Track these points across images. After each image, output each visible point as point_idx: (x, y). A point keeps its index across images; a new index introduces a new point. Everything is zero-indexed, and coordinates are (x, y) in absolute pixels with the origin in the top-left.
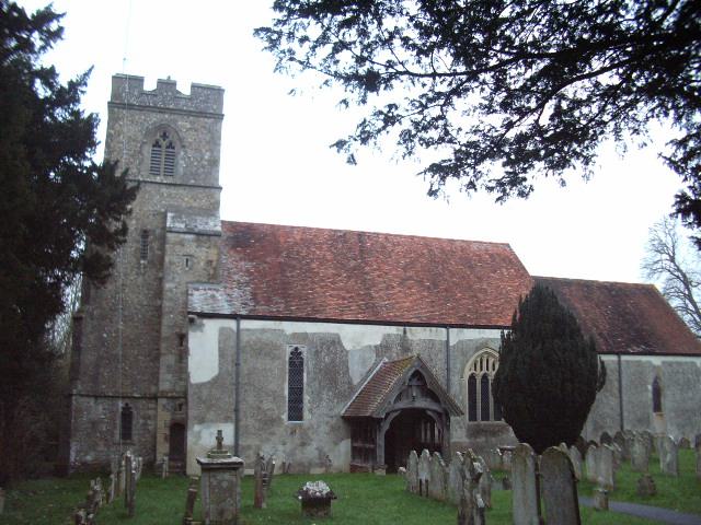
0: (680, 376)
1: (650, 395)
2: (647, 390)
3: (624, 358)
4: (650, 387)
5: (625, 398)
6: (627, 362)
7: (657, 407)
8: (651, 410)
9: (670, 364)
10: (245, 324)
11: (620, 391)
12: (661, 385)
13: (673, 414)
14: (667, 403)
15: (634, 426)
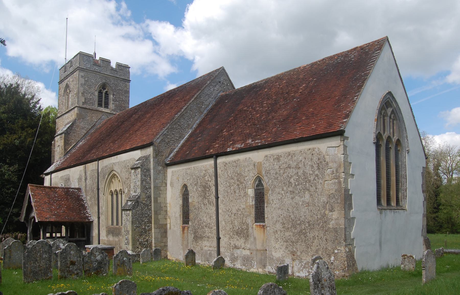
0: (292, 172)
1: (251, 202)
2: (246, 194)
3: (220, 160)
4: (251, 192)
5: (221, 206)
6: (225, 164)
7: (260, 216)
8: (250, 220)
9: (278, 158)
10: (53, 175)
11: (217, 198)
12: (266, 182)
13: (279, 226)
14: (270, 212)
15: (231, 237)
